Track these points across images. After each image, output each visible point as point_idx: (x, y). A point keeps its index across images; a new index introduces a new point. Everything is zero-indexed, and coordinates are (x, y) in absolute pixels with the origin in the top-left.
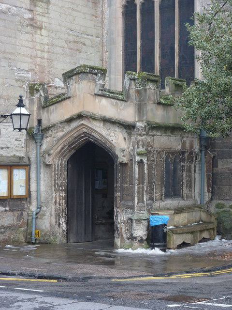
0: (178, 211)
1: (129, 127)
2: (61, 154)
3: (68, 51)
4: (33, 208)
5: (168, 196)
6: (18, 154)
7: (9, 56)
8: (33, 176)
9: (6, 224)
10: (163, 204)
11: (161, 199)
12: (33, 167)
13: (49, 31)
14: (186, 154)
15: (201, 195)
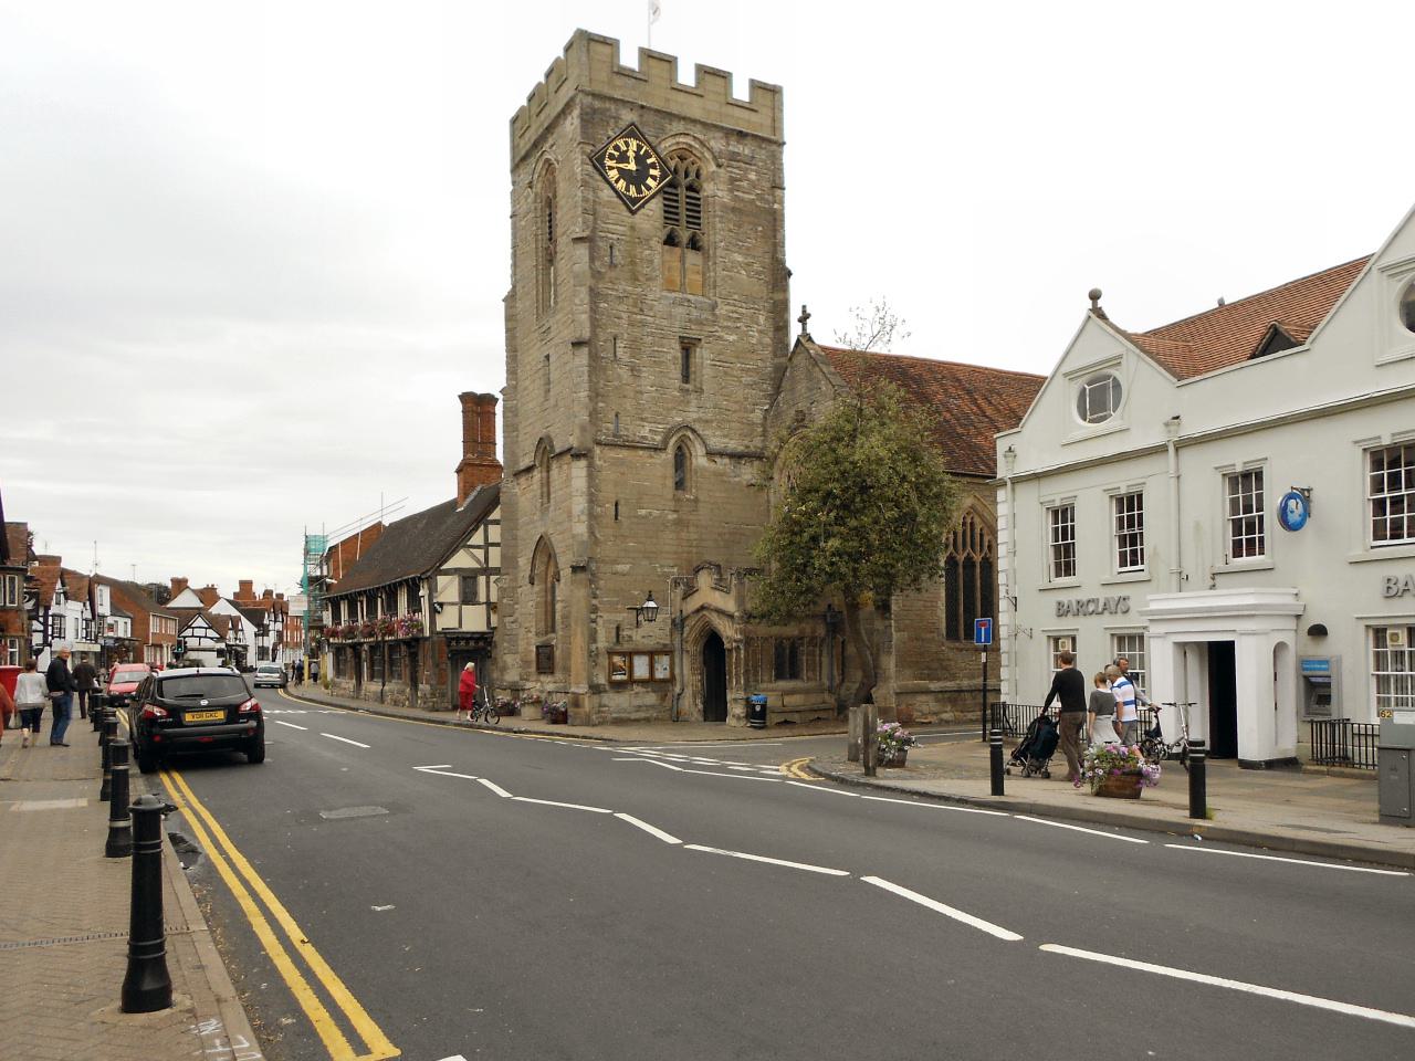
0: (792, 692)
1: (731, 616)
2: (696, 642)
3: (722, 543)
4: (677, 689)
5: (779, 676)
6: (662, 641)
7: (652, 555)
8: (677, 660)
9: (648, 703)
10: (771, 686)
11: (771, 682)
12: (677, 654)
13: (697, 526)
14: (806, 640)
15: (831, 678)
